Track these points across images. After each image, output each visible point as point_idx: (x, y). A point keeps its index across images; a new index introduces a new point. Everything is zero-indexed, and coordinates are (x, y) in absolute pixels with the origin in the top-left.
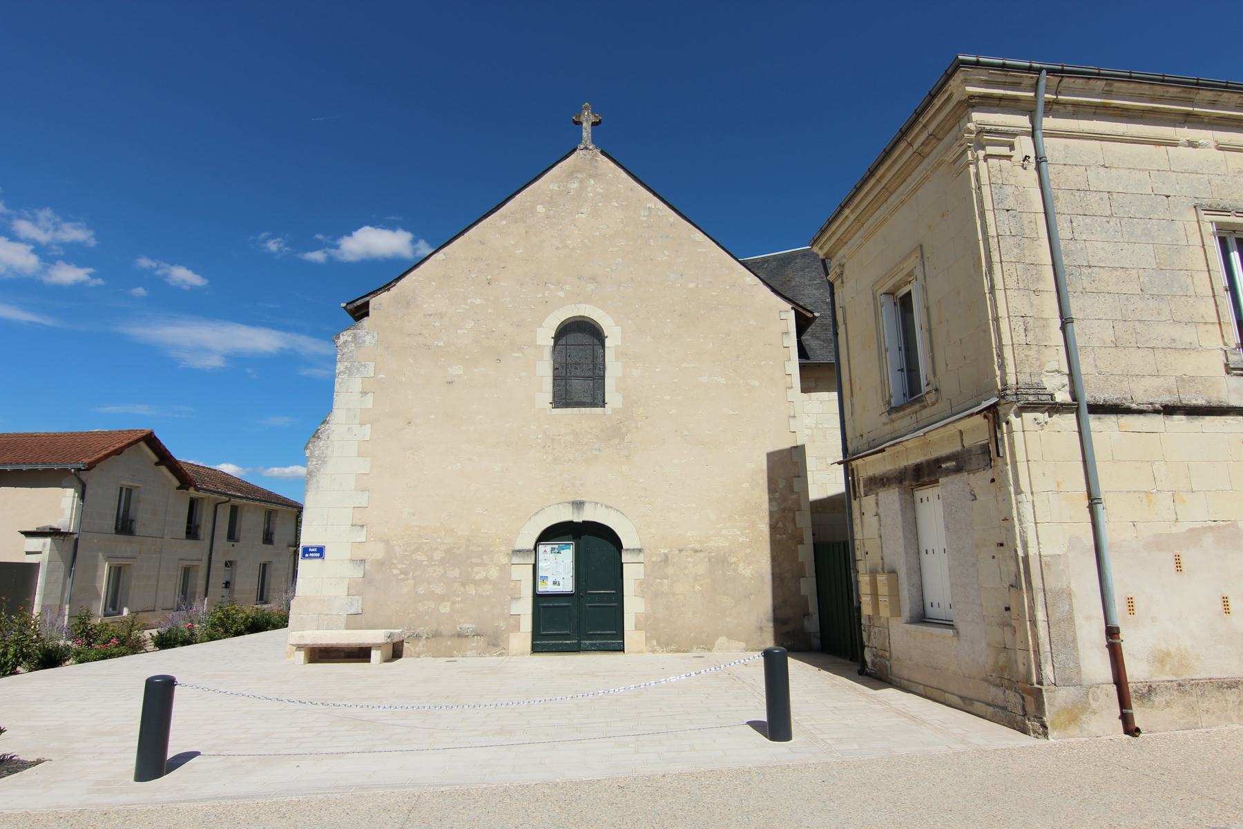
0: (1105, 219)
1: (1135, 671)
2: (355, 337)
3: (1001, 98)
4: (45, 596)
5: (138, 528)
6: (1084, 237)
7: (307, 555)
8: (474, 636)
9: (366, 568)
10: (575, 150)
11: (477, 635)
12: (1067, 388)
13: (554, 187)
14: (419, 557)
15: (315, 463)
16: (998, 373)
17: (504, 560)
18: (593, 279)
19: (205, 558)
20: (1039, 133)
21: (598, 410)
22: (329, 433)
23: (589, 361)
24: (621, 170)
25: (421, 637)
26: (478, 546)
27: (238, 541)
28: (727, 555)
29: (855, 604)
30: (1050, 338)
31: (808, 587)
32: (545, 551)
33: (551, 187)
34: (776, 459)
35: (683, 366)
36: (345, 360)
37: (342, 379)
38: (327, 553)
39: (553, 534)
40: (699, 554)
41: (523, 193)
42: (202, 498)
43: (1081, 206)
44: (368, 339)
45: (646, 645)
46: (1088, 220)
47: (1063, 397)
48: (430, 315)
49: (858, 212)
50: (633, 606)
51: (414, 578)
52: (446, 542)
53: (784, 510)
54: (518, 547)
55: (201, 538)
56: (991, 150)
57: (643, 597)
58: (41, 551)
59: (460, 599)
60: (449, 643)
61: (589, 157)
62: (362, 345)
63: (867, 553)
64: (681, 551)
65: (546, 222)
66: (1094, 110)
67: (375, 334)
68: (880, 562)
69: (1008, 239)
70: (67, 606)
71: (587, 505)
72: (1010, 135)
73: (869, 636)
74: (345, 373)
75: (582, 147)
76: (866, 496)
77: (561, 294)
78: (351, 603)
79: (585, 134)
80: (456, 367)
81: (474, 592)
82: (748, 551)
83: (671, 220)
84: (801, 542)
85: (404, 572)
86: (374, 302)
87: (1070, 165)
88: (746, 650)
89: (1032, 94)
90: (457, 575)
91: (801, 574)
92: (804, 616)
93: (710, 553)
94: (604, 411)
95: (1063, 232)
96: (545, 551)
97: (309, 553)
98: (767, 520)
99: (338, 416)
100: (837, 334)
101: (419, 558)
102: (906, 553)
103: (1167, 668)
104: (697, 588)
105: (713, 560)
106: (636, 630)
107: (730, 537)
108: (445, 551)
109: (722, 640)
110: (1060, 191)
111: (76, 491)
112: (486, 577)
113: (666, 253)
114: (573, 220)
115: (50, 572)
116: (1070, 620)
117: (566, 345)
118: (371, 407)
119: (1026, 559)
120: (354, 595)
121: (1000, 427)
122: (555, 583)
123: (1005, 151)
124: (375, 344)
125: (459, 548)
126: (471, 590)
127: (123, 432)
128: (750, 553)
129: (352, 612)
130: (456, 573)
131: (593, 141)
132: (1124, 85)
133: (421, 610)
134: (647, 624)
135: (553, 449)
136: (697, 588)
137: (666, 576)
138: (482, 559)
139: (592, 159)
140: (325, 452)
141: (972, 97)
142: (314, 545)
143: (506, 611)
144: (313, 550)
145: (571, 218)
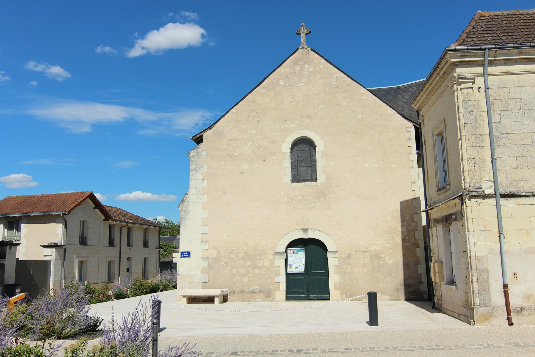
0: (517, 111)
1: (513, 301)
2: (197, 153)
3: (469, 61)
4: (55, 276)
5: (89, 242)
6: (506, 121)
7: (183, 256)
8: (259, 292)
9: (209, 261)
10: (298, 49)
11: (261, 292)
12: (493, 187)
13: (288, 70)
14: (232, 256)
15: (183, 213)
16: (463, 182)
17: (271, 257)
18: (309, 117)
19: (118, 256)
20: (486, 75)
21: (314, 183)
22: (188, 199)
23: (309, 158)
24: (321, 58)
25: (235, 293)
26: (259, 251)
27: (132, 246)
28: (380, 253)
30: (486, 167)
32: (291, 252)
33: (286, 70)
34: (405, 205)
36: (193, 164)
37: (193, 173)
38: (191, 254)
39: (294, 244)
40: (366, 253)
41: (273, 74)
42: (114, 224)
43: (505, 106)
44: (203, 153)
45: (340, 297)
46: (508, 113)
47: (490, 191)
48: (231, 140)
50: (334, 279)
51: (230, 266)
53: (409, 231)
54: (278, 251)
55: (115, 246)
56: (463, 85)
57: (338, 274)
58: (51, 255)
60: (248, 295)
61: (305, 53)
63: (434, 254)
64: (356, 252)
65: (284, 89)
66: (515, 61)
67: (206, 151)
68: (438, 257)
69: (469, 125)
70: (63, 281)
71: (310, 231)
72: (472, 80)
73: (436, 291)
75: (301, 47)
77: (293, 125)
78: (203, 277)
79: (302, 40)
80: (245, 165)
82: (391, 251)
83: (348, 82)
84: (418, 246)
85: (226, 263)
86: (205, 135)
87: (501, 88)
88: (390, 300)
89: (483, 59)
92: (420, 283)
93: (371, 252)
94: (317, 184)
95: (495, 119)
96: (291, 252)
97: (184, 255)
98: (400, 236)
99: (192, 191)
101: (233, 256)
102: (445, 254)
103: (531, 301)
105: (372, 256)
106: (335, 289)
108: (244, 253)
110: (496, 101)
111: (63, 225)
112: (263, 265)
113: (346, 100)
114: (298, 87)
115: (56, 264)
116: (487, 281)
117: (297, 151)
118: (206, 186)
119: (470, 257)
120: (205, 274)
121: (463, 204)
122: (296, 268)
123: (470, 85)
124: (206, 156)
125: (250, 252)
126: (257, 271)
127: (78, 193)
128: (391, 252)
129: (204, 281)
131: (307, 44)
132: (527, 50)
133: (235, 280)
136: (365, 270)
137: (349, 264)
139: (306, 53)
141: (455, 62)
142: (185, 251)
143: (273, 281)
144: (185, 253)
145: (297, 86)
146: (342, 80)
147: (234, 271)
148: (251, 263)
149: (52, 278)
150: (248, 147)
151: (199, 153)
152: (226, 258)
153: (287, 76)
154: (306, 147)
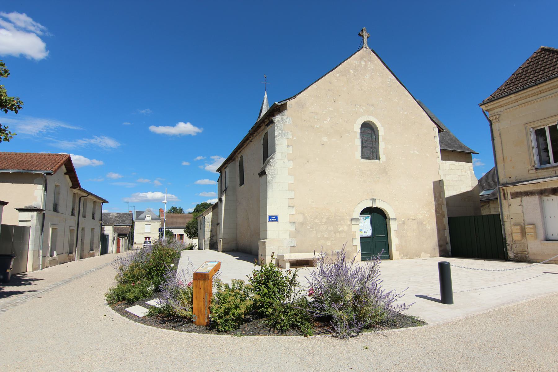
2: (282, 119)
7: (271, 220)
9: (296, 226)
10: (362, 48)
14: (317, 221)
17: (349, 223)
18: (373, 105)
19: (76, 226)
21: (378, 161)
22: (275, 164)
24: (379, 60)
26: (339, 217)
29: (504, 236)
31: (447, 233)
33: (355, 62)
35: (405, 146)
36: (279, 129)
37: (278, 139)
38: (279, 219)
44: (288, 120)
45: (400, 256)
48: (312, 113)
49: (517, 98)
50: (395, 241)
51: (316, 230)
52: (327, 214)
54: (354, 217)
55: (75, 215)
57: (397, 237)
59: (334, 239)
61: (368, 52)
62: (285, 123)
64: (408, 219)
67: (291, 119)
68: (523, 221)
70: (41, 251)
71: (377, 200)
74: (279, 136)
76: (512, 198)
77: (361, 110)
80: (325, 138)
81: (339, 236)
82: (429, 220)
84: (444, 217)
86: (290, 103)
88: (431, 257)
90: (332, 229)
91: (445, 229)
93: (418, 220)
97: (272, 219)
98: (434, 208)
100: (494, 140)
101: (317, 221)
104: (414, 234)
106: (396, 250)
107: (423, 214)
108: (326, 219)
109: (423, 254)
111: (43, 187)
112: (343, 230)
115: (36, 231)
118: (292, 153)
120: (292, 238)
122: (365, 232)
124: (291, 123)
125: (332, 218)
126: (338, 235)
129: (292, 245)
130: (331, 228)
131: (368, 45)
133: (320, 244)
134: (399, 248)
135: (363, 176)
136: (414, 234)
138: (341, 222)
140: (274, 172)
142: (273, 215)
144: (273, 217)
146: (394, 82)
147: (319, 235)
148: (333, 228)
149: (31, 247)
150: (327, 122)
151: (284, 119)
152: (312, 223)
153: (355, 67)
154: (369, 131)
